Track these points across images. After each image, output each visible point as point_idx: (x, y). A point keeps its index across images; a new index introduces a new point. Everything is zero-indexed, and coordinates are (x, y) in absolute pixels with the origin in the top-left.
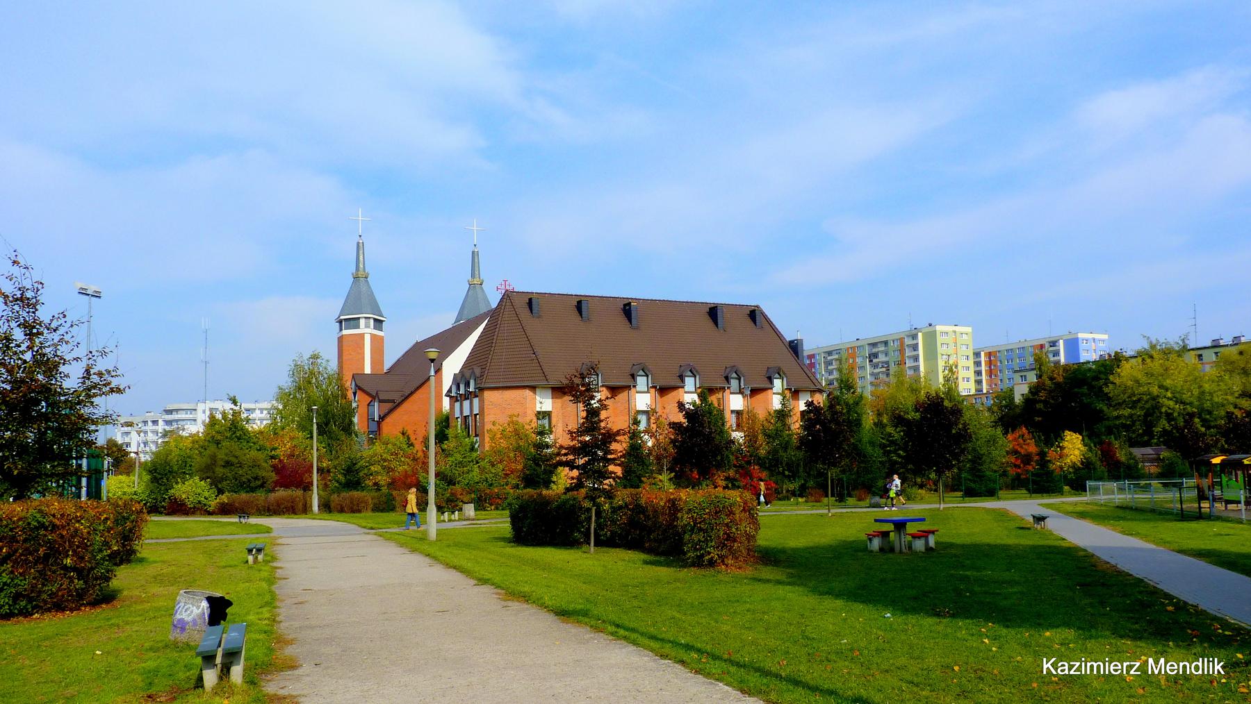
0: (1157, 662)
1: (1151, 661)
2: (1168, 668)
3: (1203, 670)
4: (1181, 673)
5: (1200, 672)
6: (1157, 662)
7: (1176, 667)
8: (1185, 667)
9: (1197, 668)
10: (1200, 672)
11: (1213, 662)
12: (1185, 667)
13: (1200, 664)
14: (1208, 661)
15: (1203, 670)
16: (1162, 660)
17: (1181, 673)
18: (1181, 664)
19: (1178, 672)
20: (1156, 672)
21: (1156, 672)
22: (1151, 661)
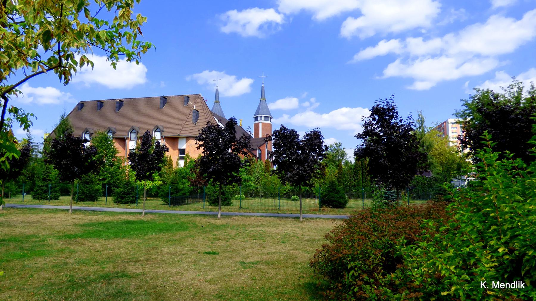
0: (496, 284)
1: (493, 282)
2: (501, 286)
3: (516, 287)
4: (506, 288)
5: (514, 287)
6: (496, 284)
7: (504, 285)
8: (508, 285)
9: (513, 285)
10: (514, 287)
11: (520, 283)
12: (508, 285)
13: (514, 284)
14: (518, 283)
15: (516, 287)
16: (498, 282)
17: (506, 288)
18: (506, 284)
19: (505, 288)
20: (496, 287)
21: (496, 287)
22: (493, 282)
